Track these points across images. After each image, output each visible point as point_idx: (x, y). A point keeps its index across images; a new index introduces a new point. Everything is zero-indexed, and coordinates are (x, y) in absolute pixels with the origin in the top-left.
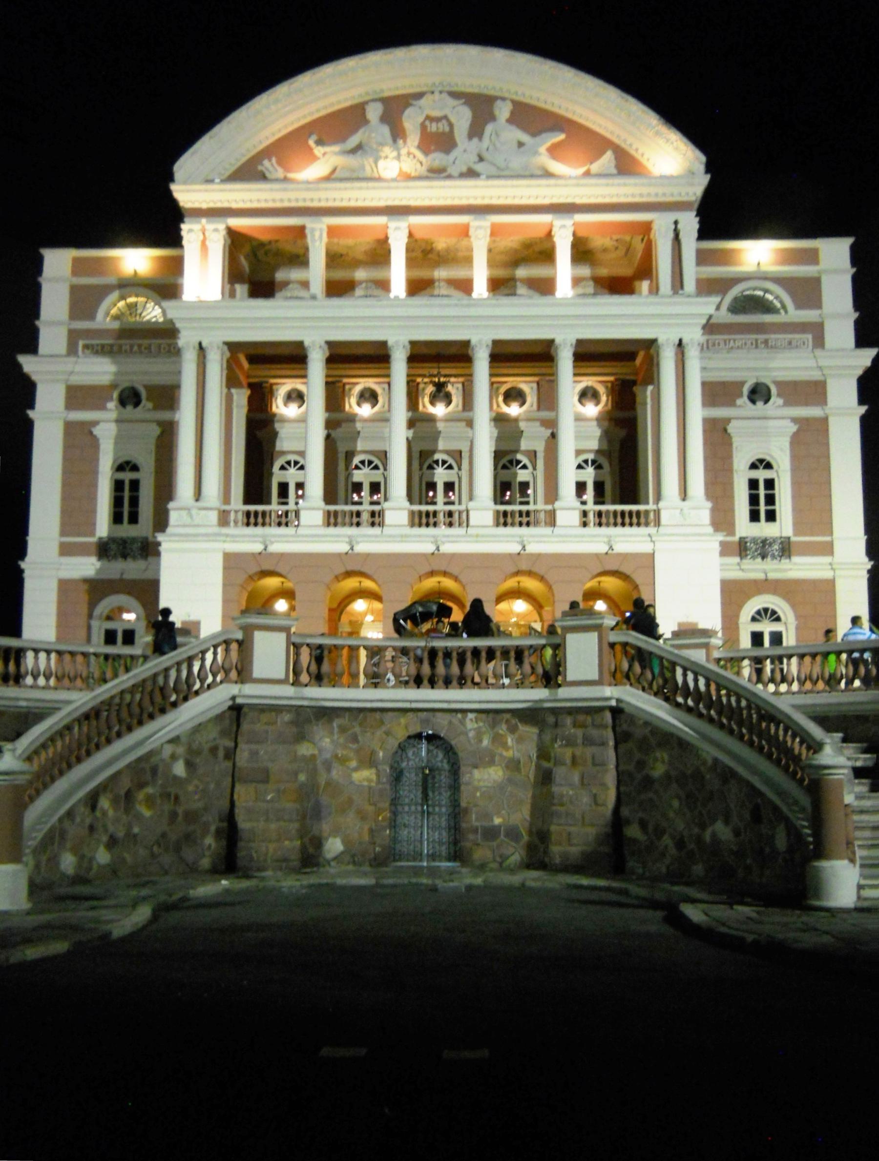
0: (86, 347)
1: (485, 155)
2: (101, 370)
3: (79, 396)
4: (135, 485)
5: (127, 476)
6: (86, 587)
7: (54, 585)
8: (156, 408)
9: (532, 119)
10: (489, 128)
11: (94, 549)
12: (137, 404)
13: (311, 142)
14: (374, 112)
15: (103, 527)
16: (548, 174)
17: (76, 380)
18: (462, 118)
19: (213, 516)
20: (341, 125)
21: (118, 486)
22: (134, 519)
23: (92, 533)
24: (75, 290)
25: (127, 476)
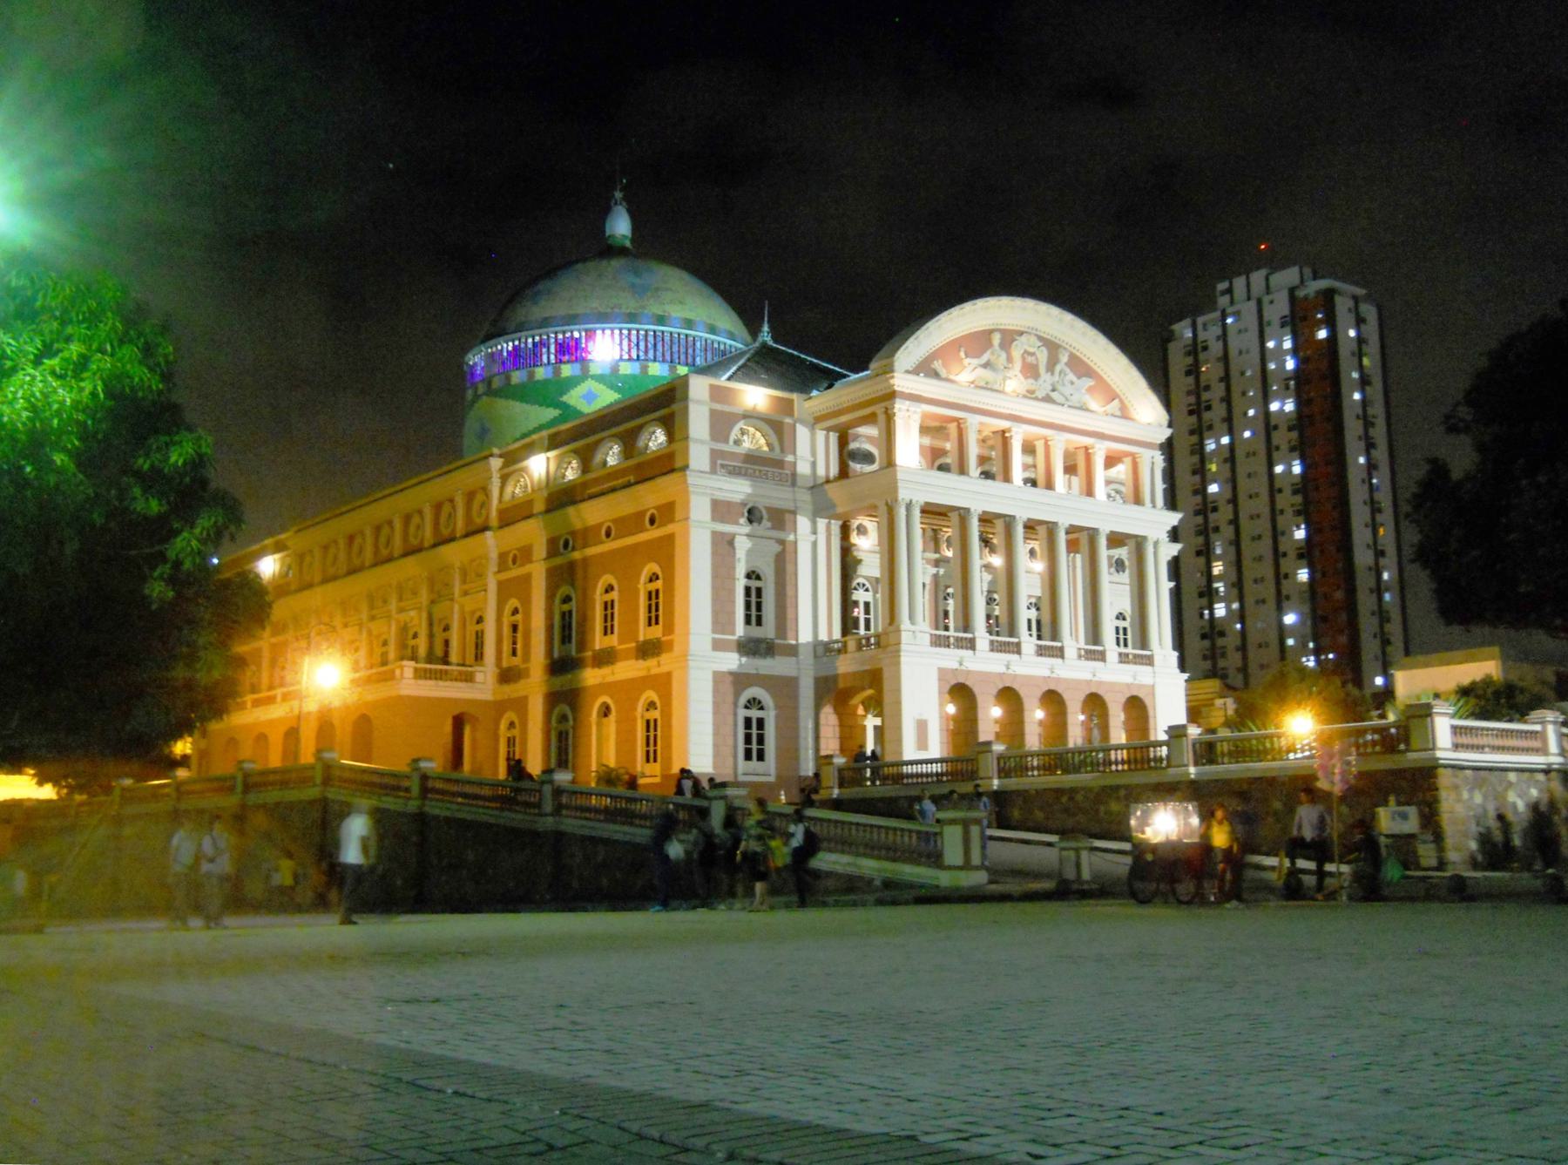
0: (722, 466)
1: (1059, 387)
2: (739, 489)
3: (721, 510)
4: (759, 591)
5: (754, 584)
6: (730, 678)
7: (710, 677)
8: (773, 528)
9: (1081, 368)
10: (1058, 368)
11: (734, 646)
12: (760, 520)
13: (962, 354)
14: (996, 339)
15: (740, 629)
16: (1083, 408)
17: (720, 496)
18: (1043, 356)
19: (927, 638)
20: (978, 342)
21: (748, 590)
22: (759, 623)
23: (733, 633)
24: (713, 413)
25: (754, 584)
